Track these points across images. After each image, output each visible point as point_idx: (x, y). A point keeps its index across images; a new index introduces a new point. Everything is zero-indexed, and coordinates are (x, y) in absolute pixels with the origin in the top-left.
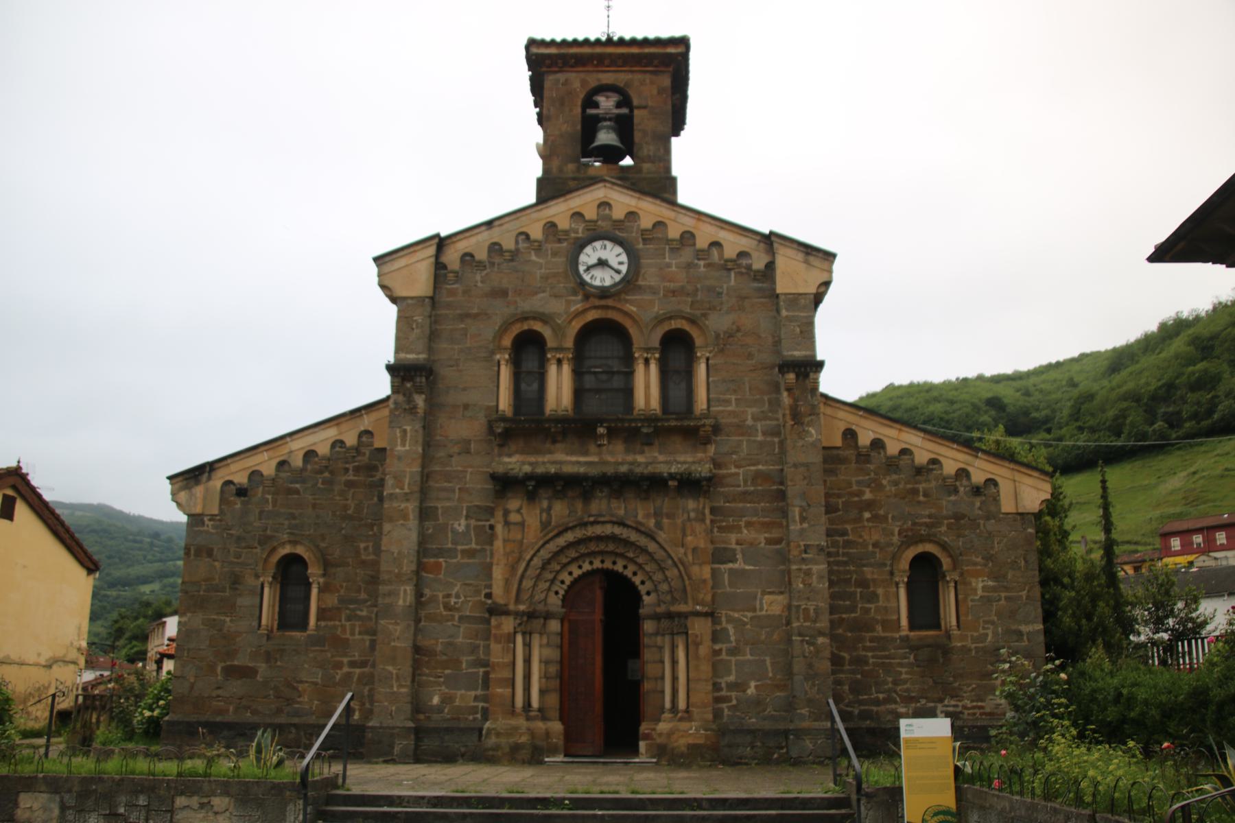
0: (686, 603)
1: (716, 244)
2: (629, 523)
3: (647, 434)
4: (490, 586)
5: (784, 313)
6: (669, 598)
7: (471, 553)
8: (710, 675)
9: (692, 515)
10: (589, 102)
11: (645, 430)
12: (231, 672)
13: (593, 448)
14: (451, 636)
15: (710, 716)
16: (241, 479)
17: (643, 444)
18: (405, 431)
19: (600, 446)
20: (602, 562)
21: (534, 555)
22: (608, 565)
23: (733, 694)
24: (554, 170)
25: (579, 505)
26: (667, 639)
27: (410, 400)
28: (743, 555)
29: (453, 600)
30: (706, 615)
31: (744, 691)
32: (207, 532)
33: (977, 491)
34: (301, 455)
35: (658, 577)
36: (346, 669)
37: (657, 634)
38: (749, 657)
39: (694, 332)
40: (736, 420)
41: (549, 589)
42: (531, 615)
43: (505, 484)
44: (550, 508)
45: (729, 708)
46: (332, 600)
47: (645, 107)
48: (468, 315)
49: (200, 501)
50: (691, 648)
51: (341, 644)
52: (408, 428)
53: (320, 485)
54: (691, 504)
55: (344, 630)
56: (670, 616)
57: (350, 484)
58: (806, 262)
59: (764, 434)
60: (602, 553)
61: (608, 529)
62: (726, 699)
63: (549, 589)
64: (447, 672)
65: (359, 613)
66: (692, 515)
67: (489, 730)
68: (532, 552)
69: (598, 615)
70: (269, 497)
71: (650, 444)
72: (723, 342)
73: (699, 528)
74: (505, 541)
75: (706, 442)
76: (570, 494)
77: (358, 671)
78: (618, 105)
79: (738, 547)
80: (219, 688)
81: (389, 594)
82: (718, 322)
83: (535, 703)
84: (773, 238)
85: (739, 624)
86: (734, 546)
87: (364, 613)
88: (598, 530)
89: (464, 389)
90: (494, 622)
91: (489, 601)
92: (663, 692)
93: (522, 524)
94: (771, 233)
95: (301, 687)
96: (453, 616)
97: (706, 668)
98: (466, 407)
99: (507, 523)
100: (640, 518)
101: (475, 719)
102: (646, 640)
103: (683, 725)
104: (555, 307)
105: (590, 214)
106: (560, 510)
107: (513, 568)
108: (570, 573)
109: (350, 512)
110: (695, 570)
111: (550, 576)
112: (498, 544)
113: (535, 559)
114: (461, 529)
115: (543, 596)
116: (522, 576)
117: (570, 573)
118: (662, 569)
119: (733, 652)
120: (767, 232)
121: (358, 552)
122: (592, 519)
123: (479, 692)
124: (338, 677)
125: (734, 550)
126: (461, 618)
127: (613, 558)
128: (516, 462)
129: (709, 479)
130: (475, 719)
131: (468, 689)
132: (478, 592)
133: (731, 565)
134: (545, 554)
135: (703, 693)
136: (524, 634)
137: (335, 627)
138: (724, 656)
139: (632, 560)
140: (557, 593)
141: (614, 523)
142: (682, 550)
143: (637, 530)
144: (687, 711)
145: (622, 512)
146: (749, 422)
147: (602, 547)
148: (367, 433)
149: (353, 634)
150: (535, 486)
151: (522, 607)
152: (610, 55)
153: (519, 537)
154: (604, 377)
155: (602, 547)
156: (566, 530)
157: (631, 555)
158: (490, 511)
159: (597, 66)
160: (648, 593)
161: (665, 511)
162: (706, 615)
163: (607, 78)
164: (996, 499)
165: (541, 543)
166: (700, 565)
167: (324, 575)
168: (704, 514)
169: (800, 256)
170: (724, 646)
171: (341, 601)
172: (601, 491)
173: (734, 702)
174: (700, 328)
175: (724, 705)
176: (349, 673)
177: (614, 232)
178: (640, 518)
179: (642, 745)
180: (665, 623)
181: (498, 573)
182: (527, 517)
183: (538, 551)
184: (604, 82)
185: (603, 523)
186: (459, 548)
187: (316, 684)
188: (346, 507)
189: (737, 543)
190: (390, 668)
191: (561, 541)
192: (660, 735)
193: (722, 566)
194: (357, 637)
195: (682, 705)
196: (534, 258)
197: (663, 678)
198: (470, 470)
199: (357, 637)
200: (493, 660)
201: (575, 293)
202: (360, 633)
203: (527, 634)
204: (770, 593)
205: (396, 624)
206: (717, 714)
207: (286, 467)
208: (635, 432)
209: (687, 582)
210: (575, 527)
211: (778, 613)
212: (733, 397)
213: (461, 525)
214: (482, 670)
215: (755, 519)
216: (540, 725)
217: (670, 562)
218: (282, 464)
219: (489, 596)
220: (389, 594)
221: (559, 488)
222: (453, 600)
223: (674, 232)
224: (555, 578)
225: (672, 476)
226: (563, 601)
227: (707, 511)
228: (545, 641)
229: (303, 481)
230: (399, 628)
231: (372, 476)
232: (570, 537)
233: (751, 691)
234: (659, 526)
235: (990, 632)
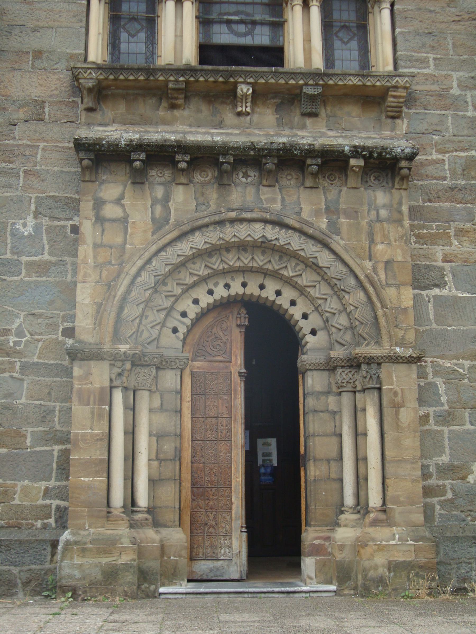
0: (378, 343)
2: (291, 222)
3: (312, 98)
4: (72, 318)
6: (348, 337)
7: (41, 268)
8: (419, 454)
9: (383, 213)
11: (309, 91)
13: (229, 117)
14: (9, 395)
15: (419, 518)
17: (304, 115)
19: (239, 114)
20: (244, 285)
21: (143, 268)
22: (253, 289)
23: (447, 482)
25: (213, 195)
26: (346, 398)
28: (454, 276)
29: (12, 339)
30: (411, 361)
31: (464, 478)
35: (333, 304)
37: (328, 393)
38: (468, 427)
40: (435, 87)
41: (163, 325)
42: (137, 361)
43: (98, 158)
44: (167, 198)
45: (441, 503)
50: (387, 411)
54: (381, 197)
56: (354, 364)
60: (243, 271)
61: (258, 231)
62: (440, 491)
63: (163, 325)
66: (383, 213)
67: (68, 542)
68: (139, 263)
69: (238, 362)
71: (314, 115)
73: (393, 232)
74: (96, 246)
75: (396, 116)
76: (198, 177)
79: (447, 265)
83: (142, 500)
85: (452, 377)
86: (440, 264)
88: (242, 232)
89: (35, 30)
90: (77, 371)
91: (70, 342)
92: (341, 480)
96: (12, 364)
97: (411, 443)
98: (38, 54)
99: (100, 220)
100: (305, 215)
101: (45, 527)
102: (311, 402)
106: (183, 200)
107: (110, 287)
108: (196, 302)
110: (390, 293)
111: (167, 303)
112: (85, 251)
113: (144, 274)
114: (28, 231)
115: (155, 333)
116: (124, 299)
117: (196, 302)
118: (338, 292)
119: (445, 419)
122: (233, 215)
123: (52, 483)
125: (443, 269)
126: (24, 367)
127: (260, 280)
128: (114, 131)
129: (411, 158)
130: (45, 527)
131: (35, 479)
132: (53, 327)
133: (436, 291)
134: (160, 266)
135: (407, 483)
136: (126, 389)
138: (432, 426)
139: (289, 282)
140: (175, 330)
141: (266, 221)
142: (368, 265)
145: (278, 206)
146: (455, 91)
147: (246, 260)
151: (123, 348)
153: (119, 240)
154: (242, 28)
155: (246, 260)
156: (192, 231)
157: (288, 273)
158: (74, 206)
160: (314, 332)
161: (342, 206)
162: (411, 361)
165: (154, 248)
166: (398, 286)
168: (400, 212)
170: (431, 410)
172: (246, 175)
173: (450, 495)
175: (435, 500)
178: (305, 215)
179: (309, 564)
180: (343, 375)
181: (85, 296)
182: (133, 213)
183: (149, 261)
185: (250, 221)
186: (24, 259)
189: (445, 260)
191: (185, 248)
192: (342, 547)
193: (424, 293)
195: (375, 500)
197: (341, 458)
198: (42, 145)
200: (76, 430)
203: (132, 392)
206: (428, 512)
208: (295, 98)
209: (380, 312)
210: (206, 226)
212: (431, 56)
213: (26, 226)
214: (57, 448)
215: (468, 226)
216: (150, 535)
217: (352, 281)
219: (70, 332)
221: (183, 165)
222: (12, 339)
224: (172, 308)
225: (357, 152)
226: (184, 341)
227: (405, 209)
228: (157, 403)
232: (199, 241)
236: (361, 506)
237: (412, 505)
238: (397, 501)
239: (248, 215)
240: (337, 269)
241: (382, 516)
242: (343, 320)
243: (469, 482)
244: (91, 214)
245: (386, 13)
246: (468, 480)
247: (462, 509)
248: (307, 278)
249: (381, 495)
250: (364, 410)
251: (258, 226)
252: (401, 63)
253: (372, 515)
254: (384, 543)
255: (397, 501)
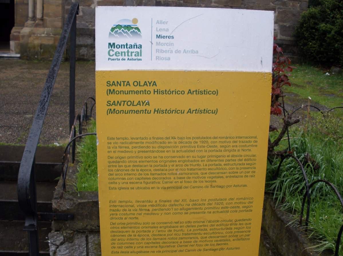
31: (89, 6)
92: (27, 4)
103: (40, 30)
144: (42, 19)
179: (12, 43)
192: (23, 36)
195: (39, 15)
236: (34, 18)
237: (56, 18)
238: (48, 15)
241: (41, 22)
243: (91, 8)
246: (91, 7)
247: (87, 21)
249: (41, 12)
253: (37, 22)
254: (39, 35)
255: (48, 15)
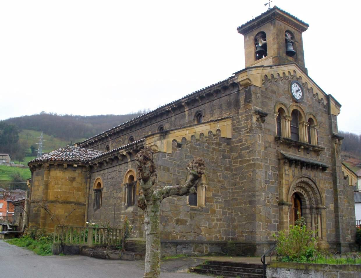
1: (317, 93)
5: (332, 120)
6: (314, 203)
10: (286, 35)
12: (178, 221)
13: (297, 151)
16: (179, 141)
18: (260, 135)
20: (298, 189)
24: (281, 54)
27: (260, 125)
32: (167, 160)
33: (345, 178)
34: (199, 133)
35: (312, 196)
36: (215, 222)
37: (309, 214)
39: (314, 120)
46: (210, 195)
47: (298, 42)
48: (267, 98)
49: (165, 146)
51: (214, 212)
52: (261, 135)
53: (205, 148)
54: (321, 174)
55: (215, 208)
56: (317, 208)
57: (214, 149)
58: (336, 106)
59: (328, 155)
61: (306, 180)
64: (269, 224)
65: (218, 200)
70: (188, 149)
71: (308, 153)
72: (320, 124)
74: (286, 180)
77: (219, 222)
78: (292, 38)
80: (174, 228)
81: (259, 196)
82: (319, 118)
84: (330, 97)
87: (220, 201)
89: (268, 124)
91: (278, 200)
93: (289, 175)
94: (330, 95)
95: (202, 228)
98: (269, 130)
99: (286, 174)
103: (322, 242)
104: (286, 102)
105: (292, 74)
109: (214, 160)
114: (270, 174)
120: (328, 94)
121: (217, 176)
122: (304, 176)
124: (213, 225)
137: (212, 205)
141: (307, 178)
143: (312, 181)
144: (322, 238)
148: (218, 130)
149: (217, 208)
150: (292, 162)
152: (292, 21)
159: (287, 23)
163: (290, 29)
164: (348, 181)
167: (208, 184)
169: (335, 104)
171: (213, 195)
174: (316, 119)
176: (217, 223)
177: (298, 81)
180: (314, 211)
181: (284, 191)
184: (289, 29)
186: (270, 180)
187: (206, 227)
188: (213, 158)
190: (260, 222)
194: (218, 209)
196: (281, 83)
199: (218, 209)
201: (290, 99)
202: (219, 208)
204: (331, 203)
205: (261, 206)
207: (193, 138)
211: (332, 209)
217: (318, 192)
218: (192, 136)
220: (259, 196)
223: (309, 87)
229: (199, 145)
230: (262, 208)
231: (220, 147)
233: (329, 232)
234: (315, 179)
235: (348, 217)
239: (306, 176)
240: (316, 189)
242: (314, 199)
244: (284, 173)
245: (316, 131)
248: (309, 190)
250: (317, 218)
251: (306, 178)
252: (319, 144)
